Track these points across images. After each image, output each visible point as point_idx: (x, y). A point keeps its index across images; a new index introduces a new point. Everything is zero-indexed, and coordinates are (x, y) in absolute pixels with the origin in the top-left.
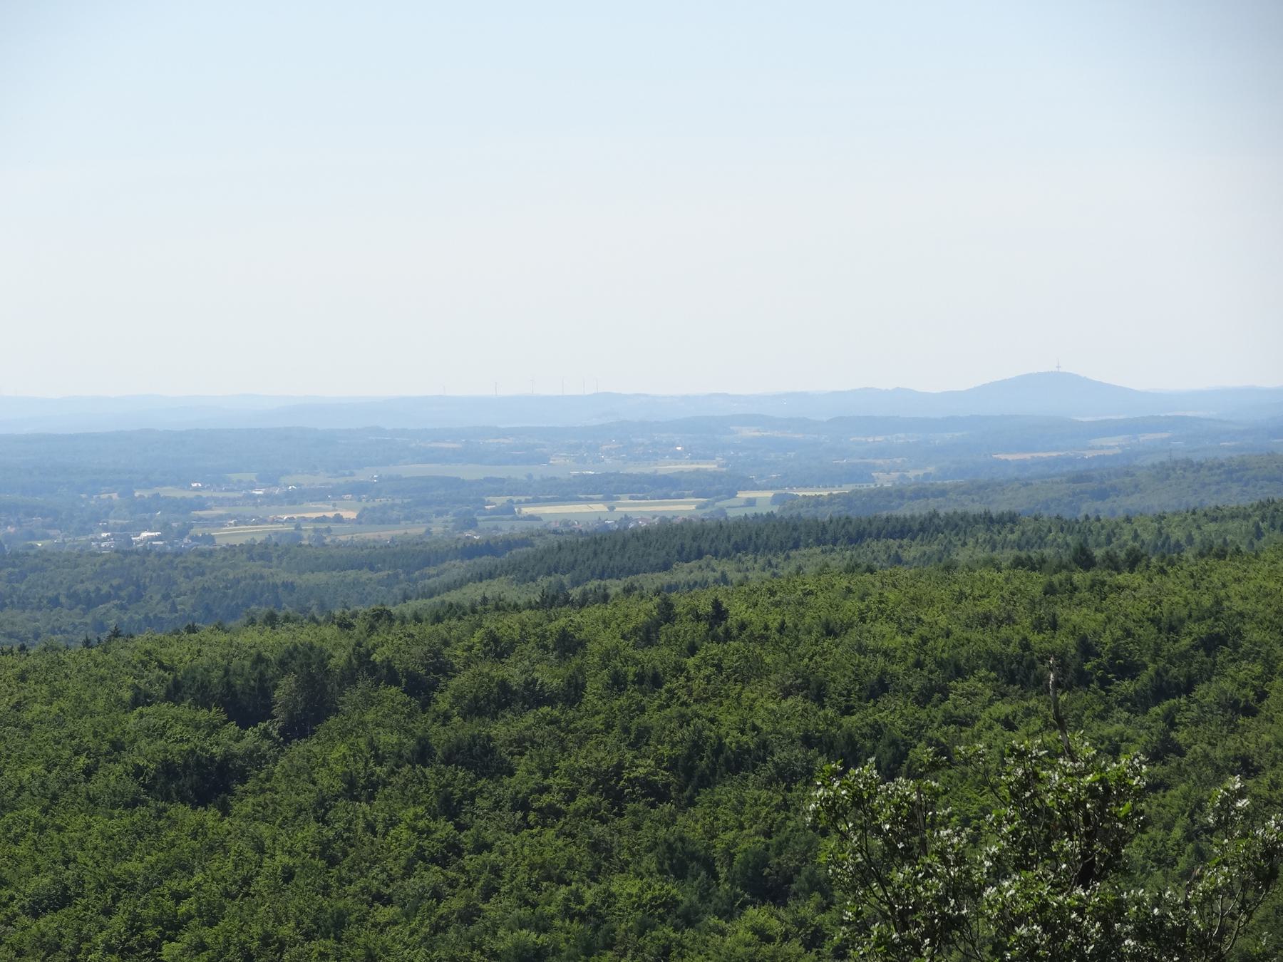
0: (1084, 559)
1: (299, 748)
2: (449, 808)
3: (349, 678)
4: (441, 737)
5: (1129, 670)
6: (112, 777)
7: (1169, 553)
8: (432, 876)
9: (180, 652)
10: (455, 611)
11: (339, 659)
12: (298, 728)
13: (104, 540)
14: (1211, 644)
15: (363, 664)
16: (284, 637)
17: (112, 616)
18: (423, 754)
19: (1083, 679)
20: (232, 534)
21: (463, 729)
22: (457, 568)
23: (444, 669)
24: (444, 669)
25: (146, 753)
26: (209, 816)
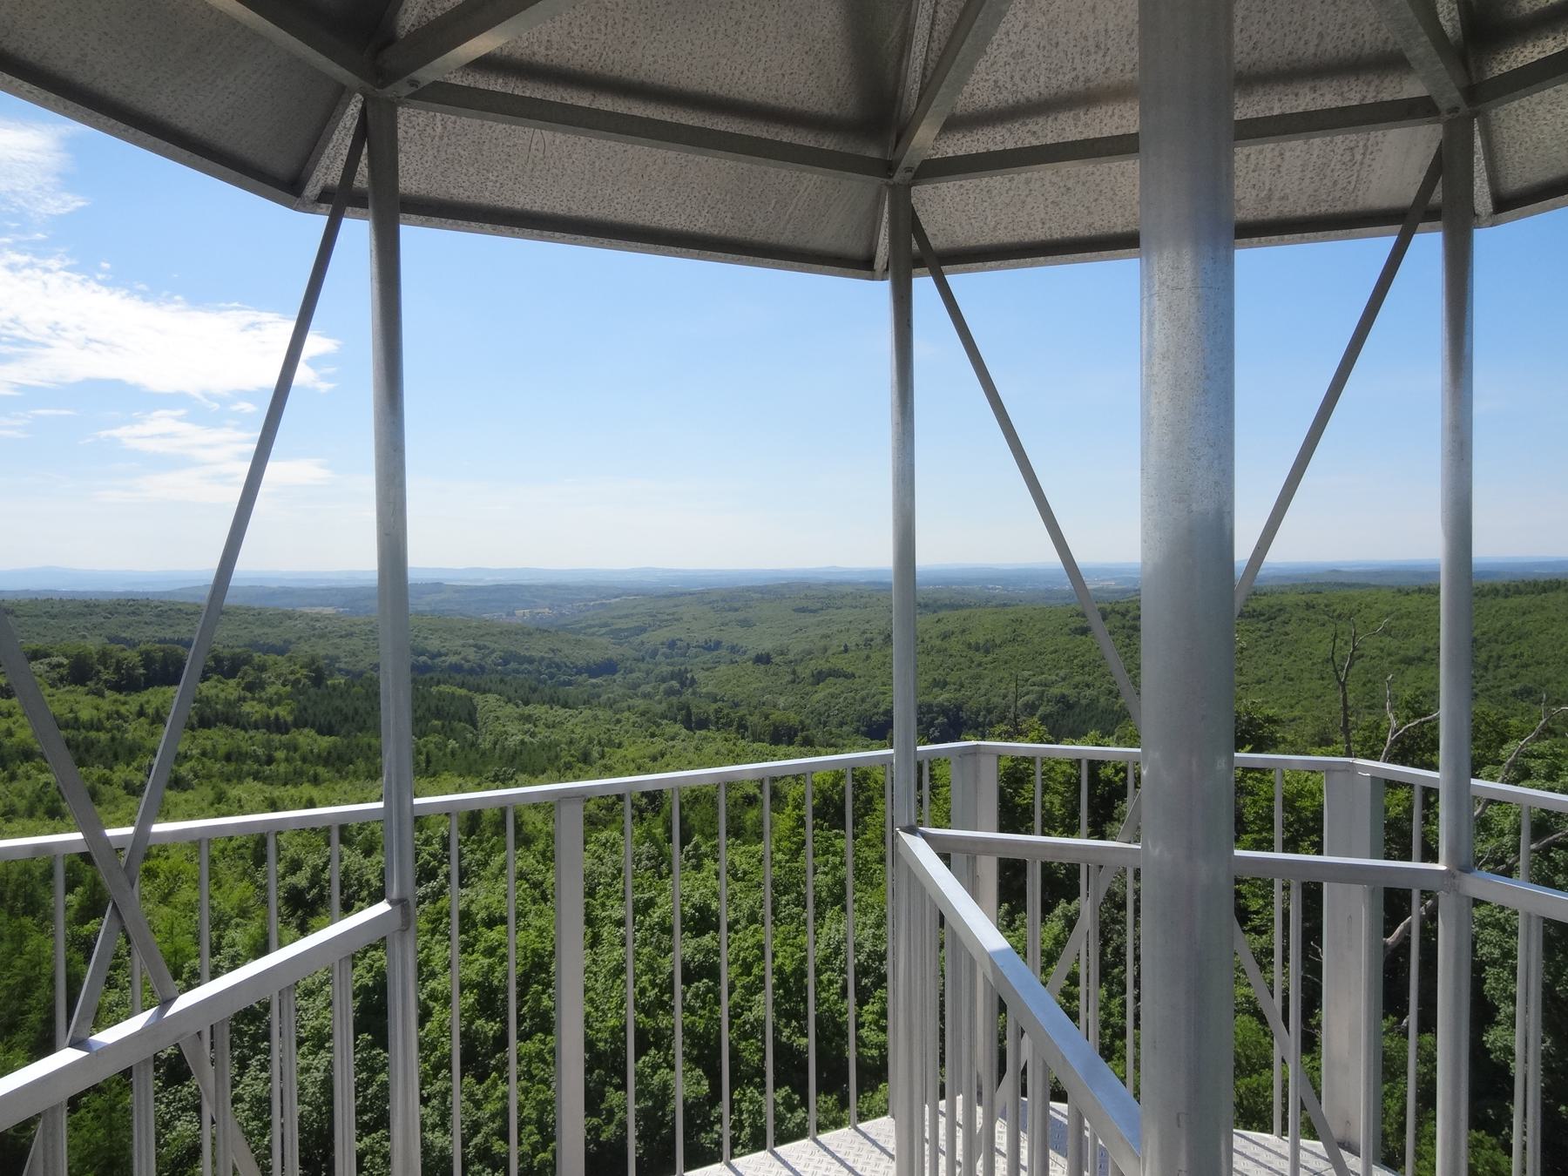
0: (1255, 594)
2: (1129, 637)
4: (1127, 624)
5: (1264, 615)
6: (1066, 630)
7: (1273, 593)
8: (1125, 649)
10: (1131, 601)
11: (1108, 610)
14: (1280, 610)
15: (1113, 611)
17: (1068, 601)
18: (1124, 627)
19: (1253, 616)
21: (1132, 623)
22: (1133, 593)
23: (1128, 611)
24: (1128, 611)
25: (1073, 626)
26: (1083, 637)
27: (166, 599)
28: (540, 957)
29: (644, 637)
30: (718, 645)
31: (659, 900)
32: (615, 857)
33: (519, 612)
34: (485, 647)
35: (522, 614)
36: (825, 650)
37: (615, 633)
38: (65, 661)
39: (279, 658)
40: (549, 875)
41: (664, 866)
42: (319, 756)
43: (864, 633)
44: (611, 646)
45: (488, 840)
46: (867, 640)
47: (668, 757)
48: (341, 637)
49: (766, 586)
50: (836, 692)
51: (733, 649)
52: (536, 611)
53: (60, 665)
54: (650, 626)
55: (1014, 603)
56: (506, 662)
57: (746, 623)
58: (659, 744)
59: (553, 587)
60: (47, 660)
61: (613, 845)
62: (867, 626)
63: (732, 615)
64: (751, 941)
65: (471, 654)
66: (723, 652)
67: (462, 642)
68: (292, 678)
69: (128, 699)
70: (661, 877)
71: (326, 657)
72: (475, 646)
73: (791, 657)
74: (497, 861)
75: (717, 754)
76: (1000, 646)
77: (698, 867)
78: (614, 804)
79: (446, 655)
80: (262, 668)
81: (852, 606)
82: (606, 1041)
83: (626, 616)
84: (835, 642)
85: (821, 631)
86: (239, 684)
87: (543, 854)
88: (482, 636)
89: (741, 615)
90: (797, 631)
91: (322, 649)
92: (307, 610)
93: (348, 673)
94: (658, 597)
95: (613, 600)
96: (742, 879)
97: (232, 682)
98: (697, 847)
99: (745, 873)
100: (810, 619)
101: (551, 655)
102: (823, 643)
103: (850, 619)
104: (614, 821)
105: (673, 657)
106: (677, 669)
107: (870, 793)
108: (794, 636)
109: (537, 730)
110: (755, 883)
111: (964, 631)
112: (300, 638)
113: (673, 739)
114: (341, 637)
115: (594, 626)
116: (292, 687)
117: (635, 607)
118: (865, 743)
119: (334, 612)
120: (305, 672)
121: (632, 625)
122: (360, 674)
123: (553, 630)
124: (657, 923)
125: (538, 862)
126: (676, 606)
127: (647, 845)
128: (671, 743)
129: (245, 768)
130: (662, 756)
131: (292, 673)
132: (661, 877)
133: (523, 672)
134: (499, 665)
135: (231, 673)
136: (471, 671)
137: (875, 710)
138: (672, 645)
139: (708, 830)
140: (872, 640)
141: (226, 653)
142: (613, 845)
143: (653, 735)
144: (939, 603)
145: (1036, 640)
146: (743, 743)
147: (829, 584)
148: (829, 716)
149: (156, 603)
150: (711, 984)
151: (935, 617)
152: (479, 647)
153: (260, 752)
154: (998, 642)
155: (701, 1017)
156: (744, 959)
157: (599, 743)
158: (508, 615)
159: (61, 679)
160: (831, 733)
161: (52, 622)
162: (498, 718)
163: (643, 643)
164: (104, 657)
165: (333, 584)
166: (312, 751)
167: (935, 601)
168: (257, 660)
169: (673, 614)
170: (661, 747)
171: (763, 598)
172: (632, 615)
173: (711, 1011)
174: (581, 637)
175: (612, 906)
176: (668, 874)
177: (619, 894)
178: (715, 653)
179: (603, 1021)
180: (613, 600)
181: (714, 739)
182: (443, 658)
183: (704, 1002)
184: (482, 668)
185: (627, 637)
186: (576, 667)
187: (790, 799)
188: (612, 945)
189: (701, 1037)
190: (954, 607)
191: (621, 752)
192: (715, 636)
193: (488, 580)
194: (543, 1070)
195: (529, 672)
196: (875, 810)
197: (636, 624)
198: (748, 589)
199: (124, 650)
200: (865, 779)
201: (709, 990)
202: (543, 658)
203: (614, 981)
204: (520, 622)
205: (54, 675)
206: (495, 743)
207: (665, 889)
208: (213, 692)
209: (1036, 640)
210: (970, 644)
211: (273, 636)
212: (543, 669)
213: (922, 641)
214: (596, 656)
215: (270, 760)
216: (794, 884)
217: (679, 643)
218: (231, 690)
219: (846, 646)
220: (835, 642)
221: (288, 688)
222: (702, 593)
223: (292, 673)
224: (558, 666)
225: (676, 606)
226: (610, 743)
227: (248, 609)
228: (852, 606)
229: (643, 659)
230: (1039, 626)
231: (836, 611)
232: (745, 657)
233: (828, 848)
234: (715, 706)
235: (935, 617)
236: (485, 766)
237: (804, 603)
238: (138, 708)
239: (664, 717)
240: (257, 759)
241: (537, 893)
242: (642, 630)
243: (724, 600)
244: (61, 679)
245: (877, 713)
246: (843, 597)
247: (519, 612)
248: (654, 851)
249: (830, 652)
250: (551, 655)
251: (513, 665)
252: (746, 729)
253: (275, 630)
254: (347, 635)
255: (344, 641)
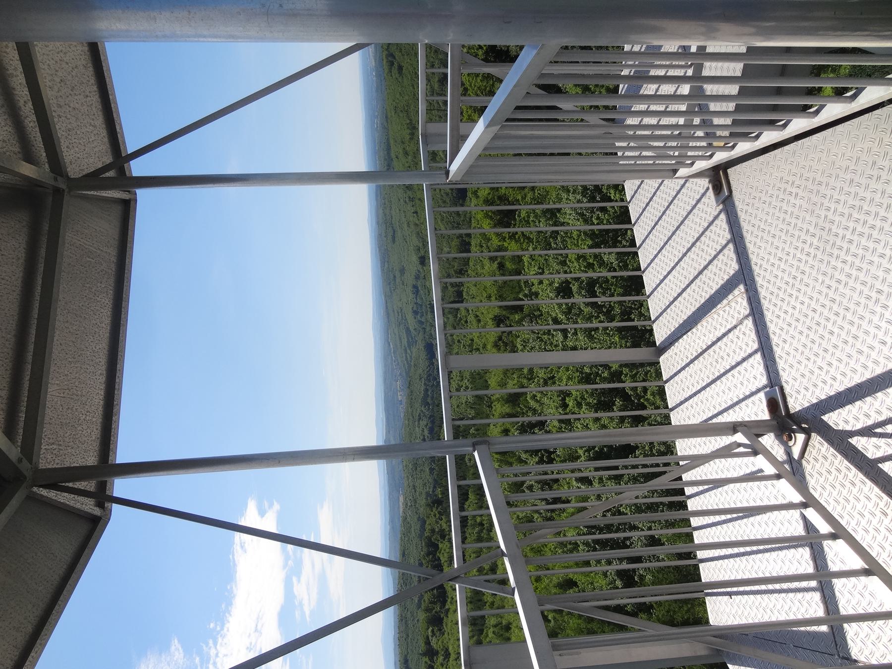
1: (397, 58)
3: (389, 51)
6: (400, 80)
9: (386, 71)
11: (387, 52)
12: (394, 58)
13: (374, 78)
16: (384, 58)
17: (383, 78)
20: (373, 63)
25: (397, 75)
26: (404, 68)
27: (397, 582)
28: (582, 378)
29: (411, 328)
30: (415, 287)
31: (554, 315)
32: (531, 341)
33: (400, 398)
34: (419, 415)
35: (401, 396)
36: (416, 225)
37: (410, 345)
38: (431, 628)
39: (427, 523)
40: (540, 376)
41: (536, 314)
42: (479, 499)
43: (406, 202)
44: (417, 347)
45: (522, 409)
46: (410, 201)
47: (478, 313)
48: (415, 491)
49: (381, 260)
50: (440, 217)
51: (417, 278)
52: (399, 389)
53: (433, 631)
54: (405, 325)
55: (385, 111)
56: (428, 404)
57: (402, 271)
58: (471, 318)
59: (385, 380)
60: (430, 638)
61: (524, 342)
62: (402, 200)
63: (398, 280)
64: (576, 264)
65: (423, 423)
66: (419, 284)
67: (417, 428)
68: (438, 516)
69: (450, 596)
70: (542, 315)
71: (427, 499)
72: (419, 421)
73: (421, 245)
74: (532, 403)
75: (476, 286)
76: (411, 120)
77: (536, 294)
78: (503, 342)
79: (424, 436)
80: (433, 531)
81: (390, 210)
82: (627, 342)
83: (400, 339)
84: (411, 219)
85: (405, 226)
86: (442, 542)
87: (529, 379)
88: (413, 418)
89: (398, 274)
90: (406, 242)
91: (422, 501)
92: (401, 510)
93: (435, 487)
94: (389, 322)
95: (392, 346)
96: (543, 269)
97: (440, 546)
98: (526, 296)
99: (539, 268)
100: (399, 234)
101: (423, 379)
102: (412, 226)
103: (398, 211)
104: (512, 342)
105: (423, 312)
106: (429, 310)
107: (496, 197)
108: (408, 243)
109: (464, 386)
110: (544, 262)
111: (403, 143)
112: (416, 512)
113: (468, 311)
114: (415, 491)
115: (406, 356)
116: (442, 515)
117: (395, 334)
118: (469, 200)
119: (402, 496)
120: (434, 509)
121: (405, 335)
122: (435, 480)
123: (409, 379)
124: (566, 316)
125: (533, 382)
126: (394, 311)
127: (524, 323)
128: (470, 312)
129: (485, 536)
130: (478, 316)
131: (435, 516)
132: (542, 315)
133: (433, 395)
134: (429, 407)
135: (436, 547)
136: (433, 422)
137: (450, 194)
138: (415, 313)
139: (517, 289)
140: (410, 197)
141: (425, 550)
142: (524, 342)
143: (466, 322)
144: (386, 157)
145: (407, 97)
146: (469, 272)
147: (378, 223)
148: (454, 222)
149: (399, 586)
150: (598, 285)
151: (395, 160)
152: (420, 419)
153: (477, 529)
154: (408, 121)
155: (615, 291)
156: (585, 267)
157: (470, 351)
158: (401, 404)
159: (440, 630)
160: (464, 221)
161: (410, 636)
162: (458, 406)
163: (415, 329)
164: (427, 610)
165: (387, 497)
166: (476, 503)
167: (385, 159)
168: (428, 534)
169: (398, 313)
170: (473, 318)
171: (388, 262)
172: (399, 335)
173: (612, 285)
174: (412, 364)
175: (557, 341)
176: (540, 311)
177: (550, 337)
178: (420, 288)
179: (616, 343)
180: (392, 346)
181: (468, 287)
182: (426, 437)
183: (607, 289)
184: (431, 416)
185: (412, 338)
186: (429, 366)
187: (499, 244)
188: (577, 339)
189: (626, 290)
190: (389, 149)
191: (476, 339)
192: (409, 289)
193: (382, 415)
194: (640, 375)
195: (432, 391)
196: (505, 194)
197: (404, 332)
198: (383, 270)
199: (424, 601)
200: (488, 201)
201: (601, 287)
202: (425, 384)
203: (595, 338)
204: (405, 397)
205: (438, 634)
206: (472, 408)
207: (548, 312)
208: (446, 555)
209: (407, 97)
210: (410, 139)
211: (416, 527)
212: (431, 384)
213: (409, 167)
214: (423, 355)
215: (481, 524)
216: (545, 241)
217: (415, 309)
218: (445, 546)
219: (413, 213)
220: (411, 219)
221: (443, 517)
222: (385, 296)
223: (435, 516)
224: (429, 375)
225: (394, 311)
226: (471, 345)
227: (402, 540)
228: (390, 210)
229: (424, 329)
230: (398, 96)
231: (394, 219)
232: (421, 270)
233: (525, 221)
234: (449, 287)
235: (395, 160)
236: (484, 412)
237: (390, 237)
238: (854, 657)
239: (456, 316)
240: (481, 531)
241: (550, 382)
242: (408, 330)
243: (389, 284)
244: (440, 630)
245: (452, 194)
246: (385, 215)
247: (400, 398)
248: (527, 319)
249: (417, 222)
250: (423, 379)
251: (429, 400)
252: (462, 269)
253: (413, 526)
254: (414, 488)
255: (418, 490)
